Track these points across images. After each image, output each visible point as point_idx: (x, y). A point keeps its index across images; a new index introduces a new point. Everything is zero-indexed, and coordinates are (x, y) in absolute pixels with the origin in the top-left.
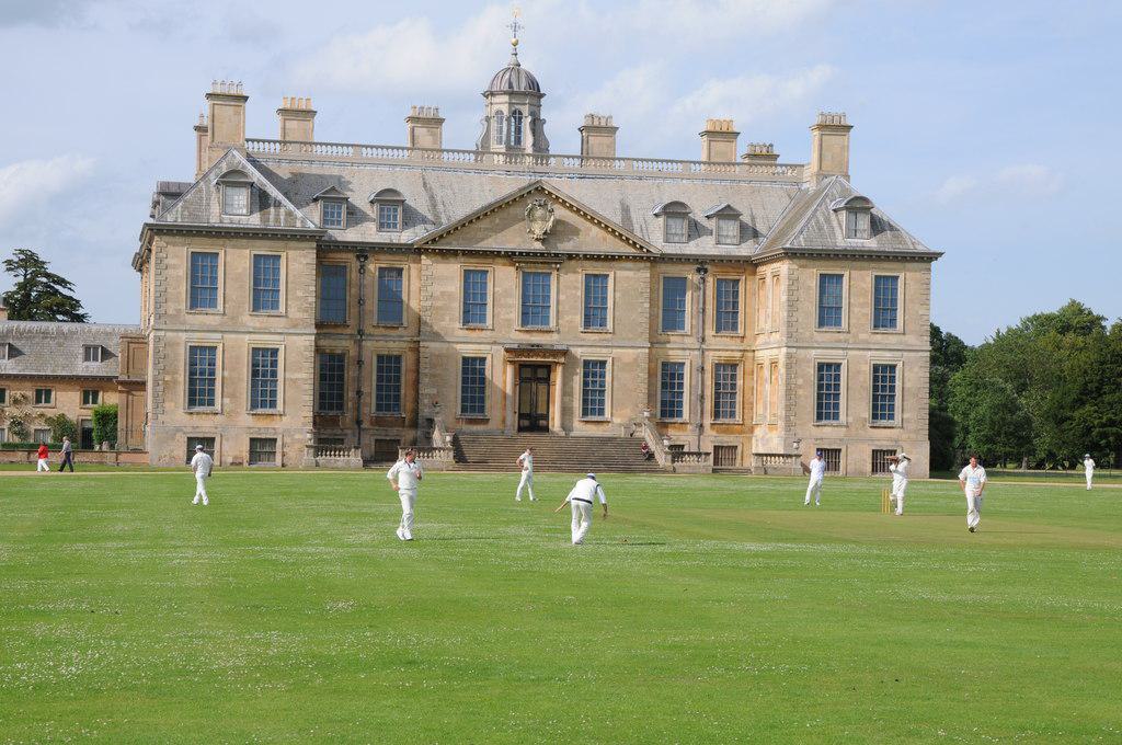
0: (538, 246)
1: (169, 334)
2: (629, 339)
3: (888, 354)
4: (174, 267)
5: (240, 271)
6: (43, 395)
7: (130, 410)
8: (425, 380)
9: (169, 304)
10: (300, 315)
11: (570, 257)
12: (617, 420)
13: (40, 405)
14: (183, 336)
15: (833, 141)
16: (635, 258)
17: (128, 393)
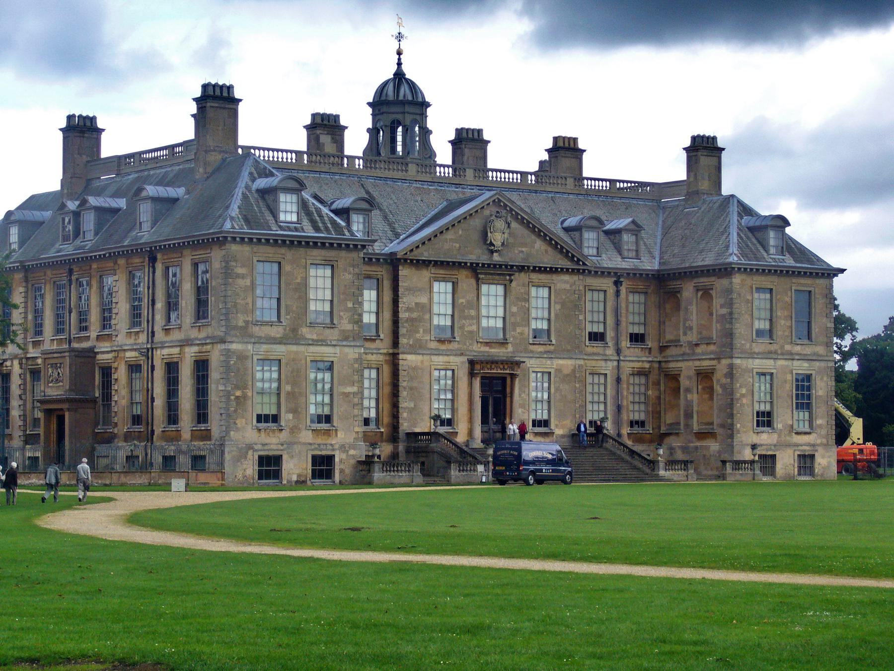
0: (496, 257)
2: (568, 351)
3: (806, 364)
4: (243, 277)
5: (299, 280)
8: (403, 394)
9: (239, 315)
10: (349, 327)
11: (522, 269)
12: (559, 432)
15: (705, 161)
16: (573, 272)
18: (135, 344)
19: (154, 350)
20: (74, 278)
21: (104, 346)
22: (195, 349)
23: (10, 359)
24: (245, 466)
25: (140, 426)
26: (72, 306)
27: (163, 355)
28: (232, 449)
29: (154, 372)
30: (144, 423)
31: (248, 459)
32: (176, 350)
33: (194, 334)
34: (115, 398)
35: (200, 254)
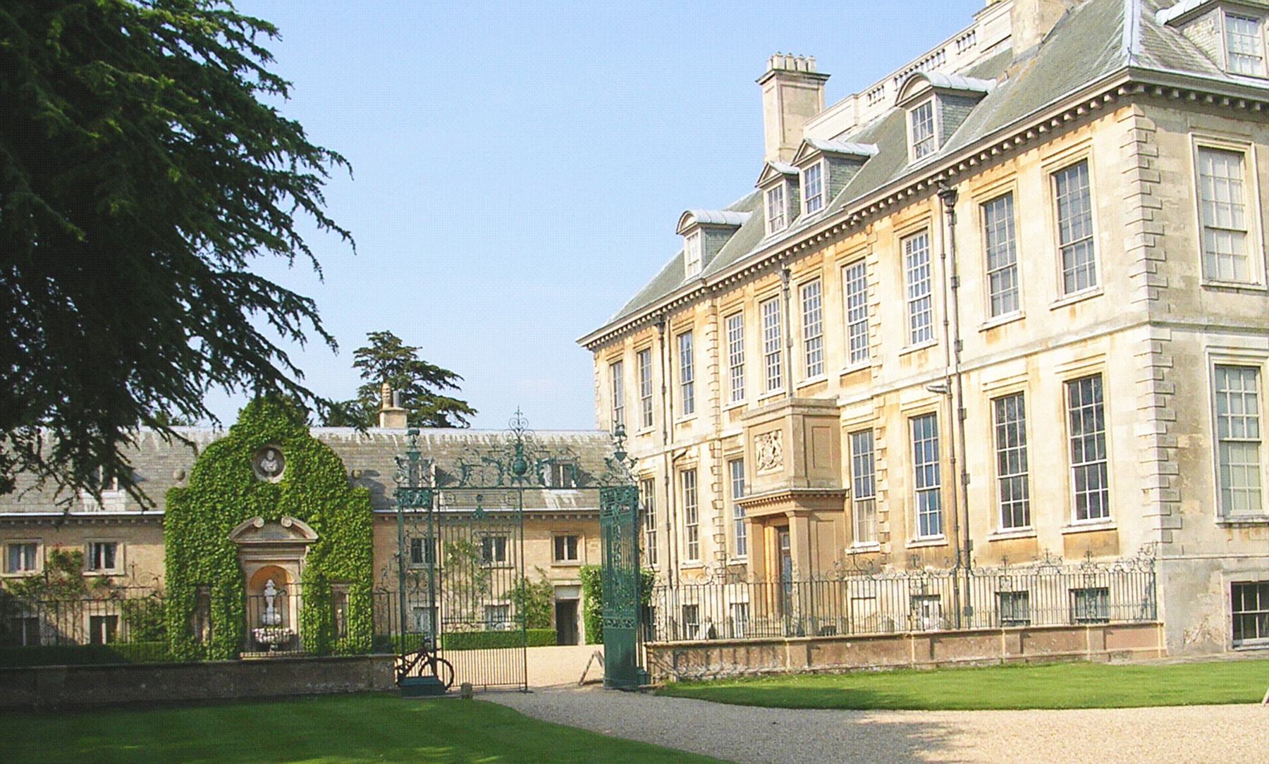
1: (1179, 336)
4: (1174, 179)
6: (492, 549)
7: (814, 551)
9: (1171, 263)
13: (562, 562)
14: (1203, 339)
17: (809, 515)
18: (920, 374)
19: (963, 377)
20: (793, 285)
21: (859, 391)
22: (1068, 354)
23: (695, 444)
24: (1205, 610)
25: (939, 536)
26: (791, 336)
27: (986, 384)
28: (1178, 570)
29: (965, 421)
30: (948, 527)
31: (1210, 591)
32: (1019, 367)
33: (1061, 323)
34: (884, 485)
35: (1062, 149)
